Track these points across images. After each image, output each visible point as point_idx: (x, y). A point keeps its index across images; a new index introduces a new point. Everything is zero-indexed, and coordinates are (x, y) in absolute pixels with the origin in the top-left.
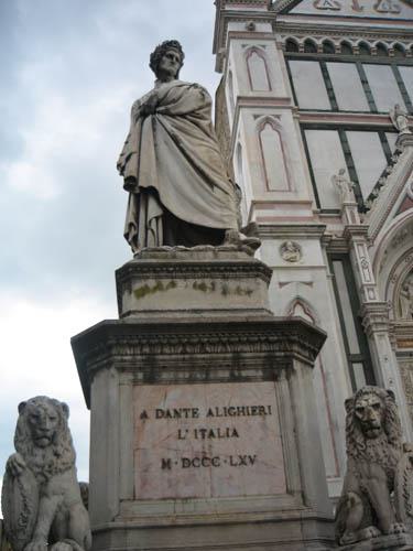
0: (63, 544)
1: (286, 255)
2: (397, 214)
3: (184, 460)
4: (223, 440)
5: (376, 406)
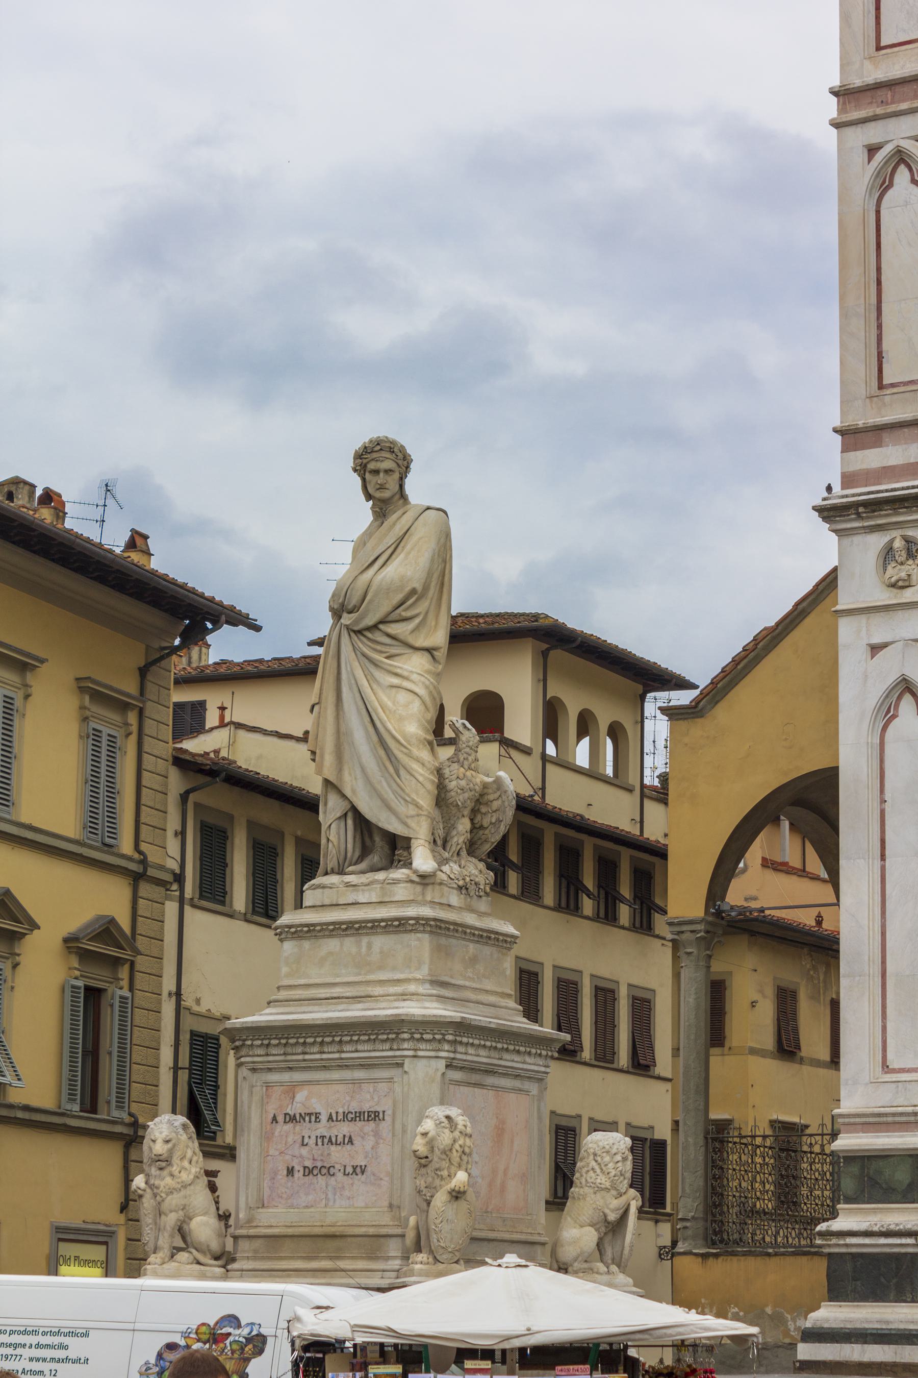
1: (894, 572)
3: (305, 1167)
4: (339, 1148)
5: (425, 1134)
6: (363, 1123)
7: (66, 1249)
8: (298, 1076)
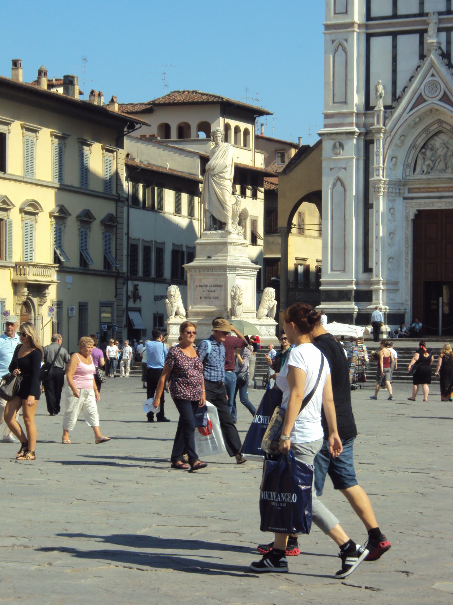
2: (411, 110)
7: (104, 309)
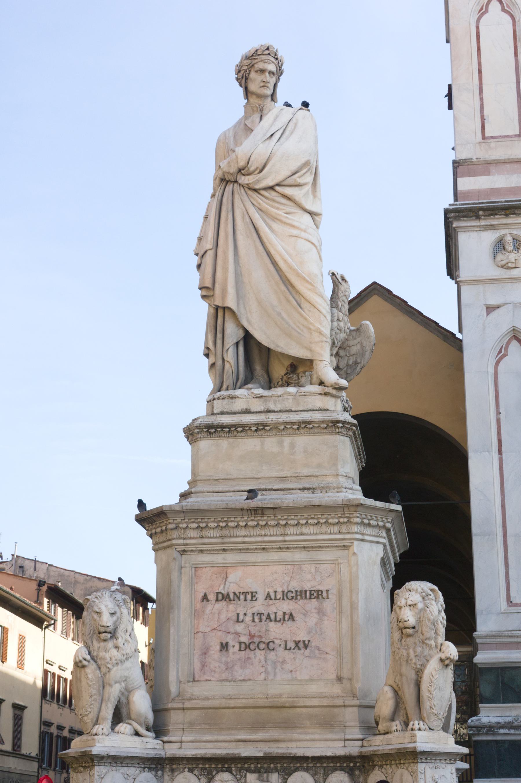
0: (125, 725)
3: (240, 643)
4: (279, 624)
5: (413, 606)
6: (305, 601)
8: (231, 558)
